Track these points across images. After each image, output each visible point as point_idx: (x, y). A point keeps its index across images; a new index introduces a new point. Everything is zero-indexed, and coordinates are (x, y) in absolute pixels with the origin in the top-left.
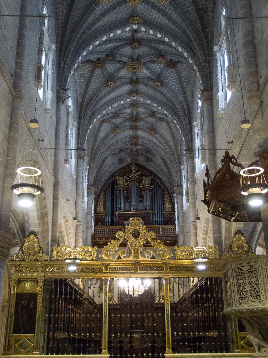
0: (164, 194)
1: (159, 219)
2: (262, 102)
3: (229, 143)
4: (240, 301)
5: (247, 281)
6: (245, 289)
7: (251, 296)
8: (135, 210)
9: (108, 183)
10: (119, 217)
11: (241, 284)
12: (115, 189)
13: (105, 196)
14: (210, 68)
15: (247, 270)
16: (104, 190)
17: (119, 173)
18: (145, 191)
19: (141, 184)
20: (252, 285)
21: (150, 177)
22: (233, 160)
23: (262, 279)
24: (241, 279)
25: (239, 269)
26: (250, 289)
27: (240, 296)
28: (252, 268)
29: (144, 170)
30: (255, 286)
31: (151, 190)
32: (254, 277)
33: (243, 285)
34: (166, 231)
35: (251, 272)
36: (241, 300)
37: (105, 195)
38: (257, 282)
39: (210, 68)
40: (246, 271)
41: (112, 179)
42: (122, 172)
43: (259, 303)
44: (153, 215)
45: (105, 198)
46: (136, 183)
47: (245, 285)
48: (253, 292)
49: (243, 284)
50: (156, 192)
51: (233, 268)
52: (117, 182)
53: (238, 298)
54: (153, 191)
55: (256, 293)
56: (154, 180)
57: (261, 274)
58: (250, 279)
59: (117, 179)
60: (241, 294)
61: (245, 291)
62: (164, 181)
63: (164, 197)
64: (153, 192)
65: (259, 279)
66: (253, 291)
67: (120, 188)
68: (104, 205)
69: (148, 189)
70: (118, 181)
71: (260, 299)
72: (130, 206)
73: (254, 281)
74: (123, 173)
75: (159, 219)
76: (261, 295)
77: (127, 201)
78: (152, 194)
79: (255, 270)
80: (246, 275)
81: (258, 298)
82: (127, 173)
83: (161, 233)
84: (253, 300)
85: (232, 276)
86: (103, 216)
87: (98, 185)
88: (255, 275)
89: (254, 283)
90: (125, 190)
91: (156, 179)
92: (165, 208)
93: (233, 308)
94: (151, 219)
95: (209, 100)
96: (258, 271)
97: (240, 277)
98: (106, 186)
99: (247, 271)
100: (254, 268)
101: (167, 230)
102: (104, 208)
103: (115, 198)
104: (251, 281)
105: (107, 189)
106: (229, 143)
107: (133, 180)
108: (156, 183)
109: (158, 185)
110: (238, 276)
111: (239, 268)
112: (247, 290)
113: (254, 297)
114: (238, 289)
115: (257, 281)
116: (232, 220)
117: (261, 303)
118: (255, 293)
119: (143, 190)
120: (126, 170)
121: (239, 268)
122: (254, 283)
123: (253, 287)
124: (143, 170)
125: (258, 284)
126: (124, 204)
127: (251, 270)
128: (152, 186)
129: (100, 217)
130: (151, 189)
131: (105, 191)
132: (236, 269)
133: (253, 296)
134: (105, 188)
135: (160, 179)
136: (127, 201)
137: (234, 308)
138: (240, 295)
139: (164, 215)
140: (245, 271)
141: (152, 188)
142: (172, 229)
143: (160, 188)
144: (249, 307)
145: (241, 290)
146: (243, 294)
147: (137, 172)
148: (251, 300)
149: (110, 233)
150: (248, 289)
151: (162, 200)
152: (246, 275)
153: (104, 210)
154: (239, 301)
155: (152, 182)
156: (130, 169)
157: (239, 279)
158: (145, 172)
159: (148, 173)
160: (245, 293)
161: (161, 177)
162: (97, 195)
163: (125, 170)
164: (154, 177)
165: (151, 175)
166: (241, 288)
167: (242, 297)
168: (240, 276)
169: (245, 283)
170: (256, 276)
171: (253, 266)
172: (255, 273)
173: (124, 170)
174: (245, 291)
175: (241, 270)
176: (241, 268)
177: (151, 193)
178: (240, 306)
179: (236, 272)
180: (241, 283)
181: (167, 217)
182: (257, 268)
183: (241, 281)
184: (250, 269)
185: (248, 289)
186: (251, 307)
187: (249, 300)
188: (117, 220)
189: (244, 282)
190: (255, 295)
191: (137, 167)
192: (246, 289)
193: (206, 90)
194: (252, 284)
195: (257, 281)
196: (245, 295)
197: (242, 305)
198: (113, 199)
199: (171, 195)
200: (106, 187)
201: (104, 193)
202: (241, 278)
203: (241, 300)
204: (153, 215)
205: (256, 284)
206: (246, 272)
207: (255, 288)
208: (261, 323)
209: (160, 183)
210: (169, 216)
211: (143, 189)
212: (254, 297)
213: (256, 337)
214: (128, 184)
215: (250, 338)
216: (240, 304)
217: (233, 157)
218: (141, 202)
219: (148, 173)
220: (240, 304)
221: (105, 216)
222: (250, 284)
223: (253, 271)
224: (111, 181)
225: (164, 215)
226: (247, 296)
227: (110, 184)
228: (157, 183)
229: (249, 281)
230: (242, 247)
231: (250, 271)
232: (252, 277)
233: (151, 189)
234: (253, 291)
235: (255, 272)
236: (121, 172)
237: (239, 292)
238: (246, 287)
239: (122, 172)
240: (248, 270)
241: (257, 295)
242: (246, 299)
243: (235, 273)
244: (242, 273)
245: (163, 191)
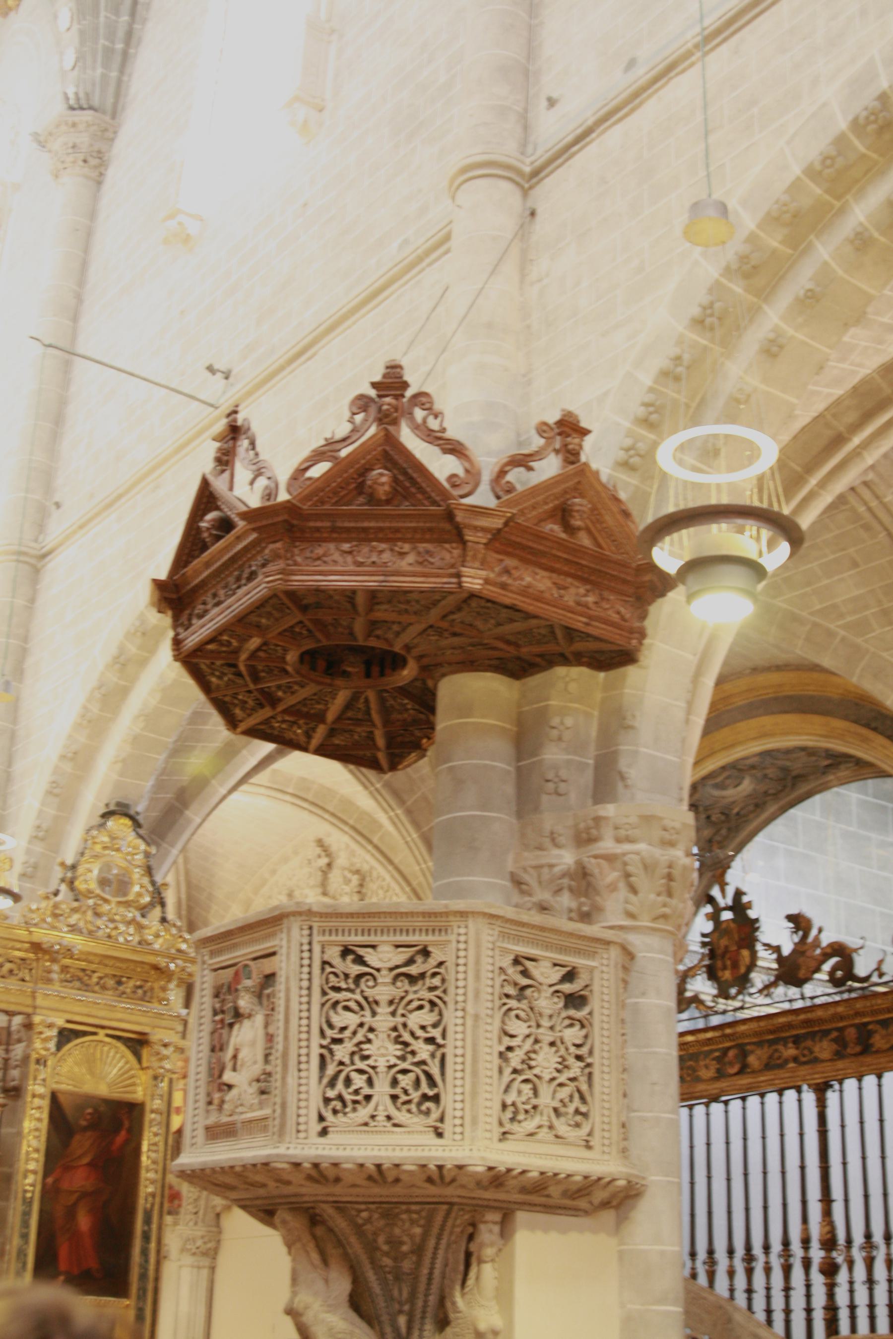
2: (533, 214)
3: (211, 369)
4: (328, 1115)
5: (383, 1021)
6: (366, 1058)
7: (394, 1098)
11: (347, 1033)
14: (133, 14)
15: (391, 964)
20: (406, 1044)
22: (419, 414)
23: (469, 1022)
24: (347, 1008)
25: (350, 957)
26: (393, 1061)
27: (331, 1094)
28: (419, 959)
30: (424, 1051)
32: (421, 1007)
33: (360, 1037)
35: (413, 979)
36: (335, 1112)
38: (436, 1033)
39: (133, 14)
40: (384, 972)
43: (430, 1138)
47: (369, 1041)
48: (406, 1081)
49: (355, 1033)
51: (317, 949)
53: (315, 1102)
55: (425, 1088)
57: (470, 995)
58: (400, 1011)
60: (340, 1085)
61: (361, 1072)
65: (451, 1017)
66: (405, 1072)
71: (442, 1120)
73: (423, 1028)
76: (447, 1099)
79: (434, 975)
80: (383, 991)
81: (428, 1113)
84: (401, 1116)
85: (305, 984)
88: (430, 996)
89: (419, 1033)
93: (282, 1150)
95: (93, 162)
96: (451, 977)
97: (349, 995)
99: (391, 969)
100: (432, 961)
104: (405, 1025)
106: (211, 369)
110: (337, 989)
111: (346, 952)
112: (374, 1068)
113: (409, 1102)
114: (322, 1057)
115: (435, 1026)
116: (251, 722)
117: (440, 1135)
118: (417, 1083)
121: (346, 952)
122: (419, 1033)
123: (413, 1053)
125: (440, 1040)
127: (413, 970)
132: (333, 954)
133: (404, 1098)
137: (291, 1152)
138: (332, 1084)
140: (378, 970)
145: (341, 1063)
146: (348, 1082)
148: (389, 1118)
150: (382, 1064)
152: (383, 991)
154: (321, 1118)
157: (337, 1003)
160: (359, 1081)
166: (342, 1052)
167: (340, 1097)
168: (348, 990)
169: (371, 1030)
170: (433, 1004)
171: (425, 953)
172: (432, 989)
174: (361, 1072)
175: (360, 960)
176: (361, 951)
178: (322, 1140)
179: (328, 969)
180: (343, 1029)
182: (450, 964)
183: (350, 1019)
184: (410, 961)
185: (382, 1064)
186: (390, 1153)
187: (381, 1118)
189: (361, 1025)
190: (415, 1096)
192: (371, 1062)
193: (91, 108)
194: (407, 1037)
195: (435, 1026)
196: (356, 1092)
197: (331, 1138)
202: (352, 1004)
203: (335, 1112)
205: (430, 1040)
206: (385, 977)
207: (424, 1062)
208: (381, 1239)
212: (409, 1102)
213: (332, 1308)
215: (307, 1308)
216: (324, 1132)
217: (422, 399)
220: (324, 1132)
222: (398, 1040)
223: (422, 976)
226: (368, 1098)
229: (391, 1022)
230: (122, 885)
231: (407, 976)
232: (415, 1004)
234: (405, 1072)
235: (436, 981)
237: (331, 1069)
238: (368, 1049)
240: (397, 967)
241: (425, 1097)
242: (363, 1113)
243: (323, 969)
244: (359, 976)
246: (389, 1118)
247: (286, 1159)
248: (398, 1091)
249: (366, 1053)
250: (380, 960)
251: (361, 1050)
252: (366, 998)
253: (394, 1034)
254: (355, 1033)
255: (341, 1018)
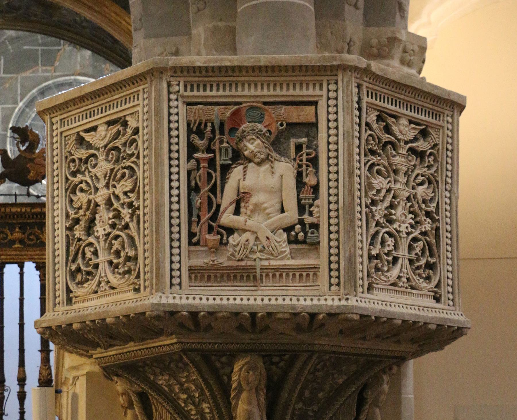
6: (391, 222)
7: (411, 261)
24: (379, 172)
36: (377, 269)
99: (406, 143)
104: (415, 196)
110: (373, 152)
112: (398, 232)
121: (379, 118)
122: (423, 206)
132: (372, 117)
144: (405, 311)
146: (383, 242)
176: (391, 120)
179: (369, 132)
180: (378, 191)
185: (403, 228)
189: (389, 191)
216: (370, 288)
220: (370, 288)
234: (415, 240)
246: (408, 279)
247: (360, 312)
248: (413, 256)
249: (394, 217)
250: (401, 132)
251: (391, 214)
252: (390, 165)
253: (409, 204)
254: (384, 197)
255: (379, 182)
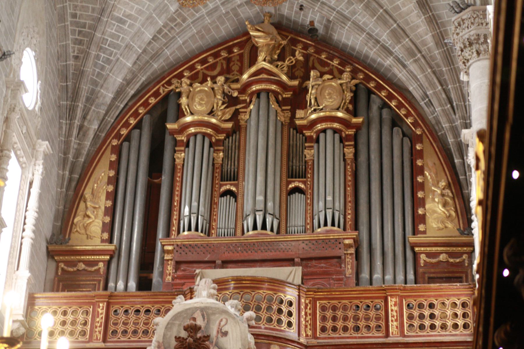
0: (420, 154)
1: (389, 277)
8: (264, 227)
9: (136, 114)
10: (178, 263)
12: (168, 139)
13: (118, 173)
16: (115, 142)
17: (192, 68)
18: (317, 141)
19: (300, 113)
21: (346, 76)
29: (318, 52)
31: (348, 138)
34: (422, 317)
37: (116, 166)
41: (156, 94)
42: (211, 60)
44: (358, 256)
45: (114, 181)
46: (274, 106)
50: (374, 146)
52: (179, 106)
54: (362, 140)
56: (370, 92)
59: (179, 95)
62: (417, 94)
63: (421, 171)
64: (362, 148)
67: (192, 130)
68: (111, 212)
69: (335, 131)
70: (184, 100)
72: (240, 216)
74: (213, 67)
75: (389, 277)
77: (229, 193)
78: (356, 155)
82: (235, 68)
83: (393, 326)
86: (96, 263)
87: (84, 118)
90: (219, 142)
91: (380, 87)
92: (423, 219)
94: (349, 270)
98: (127, 124)
101: (427, 312)
102: (109, 228)
103: (165, 179)
105: (128, 138)
107: (258, 93)
108: (375, 108)
109: (385, 112)
119: (308, 139)
120: (229, 50)
124: (311, 50)
126: (212, 205)
128: (355, 115)
129: (82, 266)
130: (351, 132)
131: (118, 151)
134: (118, 136)
135: (402, 90)
136: (229, 193)
139: (416, 255)
141: (358, 127)
142: (455, 305)
143: (395, 129)
147: (282, 58)
149: (111, 328)
151: (407, 164)
153: (106, 236)
155: (354, 100)
156: (246, 51)
158: (323, 56)
159: (335, 62)
161: (401, 75)
162: (78, 170)
163: (224, 54)
164: (368, 79)
165: (354, 73)
173: (216, 55)
177: (349, 152)
181: (433, 265)
188: (169, 279)
191: (284, 37)
198: (158, 187)
199: (457, 161)
200: (124, 132)
201: (114, 158)
204: (358, 256)
209: (400, 106)
210: (443, 257)
211: (308, 133)
214: (236, 113)
218: (297, 197)
219: (335, 62)
221: (108, 264)
224: (153, 101)
225: (416, 255)
227: (147, 118)
228: (385, 105)
233: (351, 132)
236: (203, 62)
239: (211, 60)
245: (414, 139)
